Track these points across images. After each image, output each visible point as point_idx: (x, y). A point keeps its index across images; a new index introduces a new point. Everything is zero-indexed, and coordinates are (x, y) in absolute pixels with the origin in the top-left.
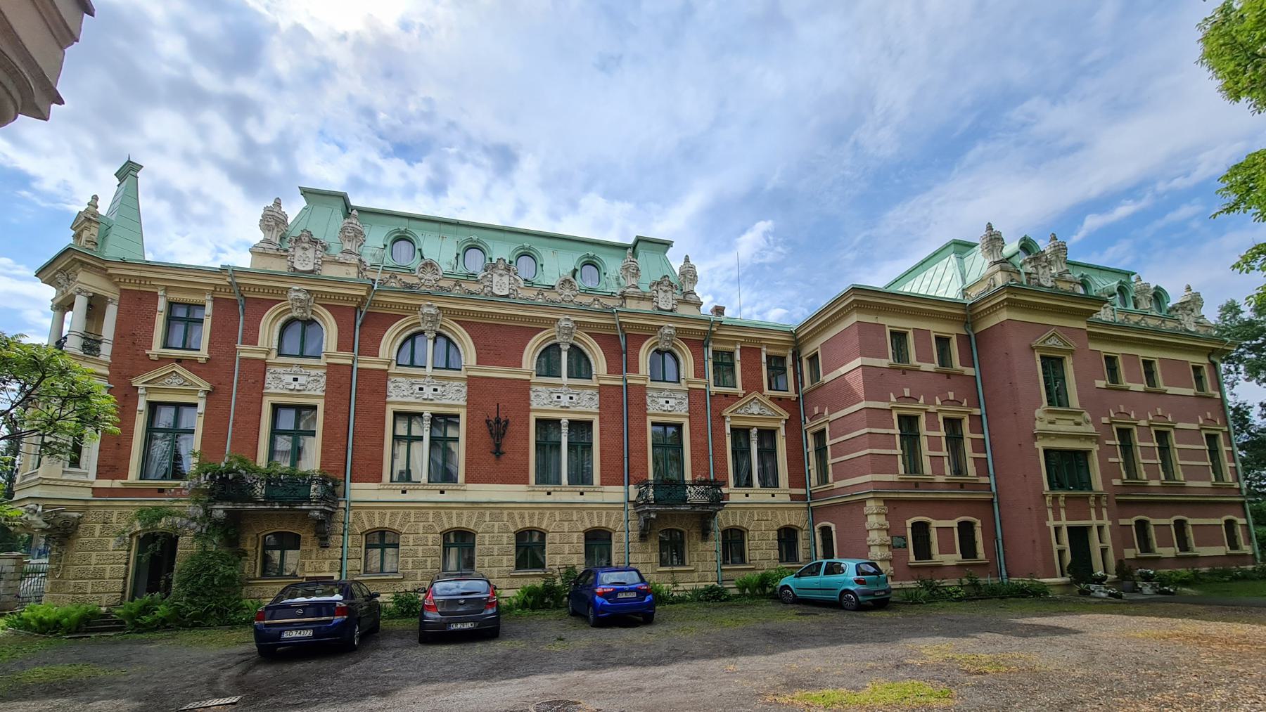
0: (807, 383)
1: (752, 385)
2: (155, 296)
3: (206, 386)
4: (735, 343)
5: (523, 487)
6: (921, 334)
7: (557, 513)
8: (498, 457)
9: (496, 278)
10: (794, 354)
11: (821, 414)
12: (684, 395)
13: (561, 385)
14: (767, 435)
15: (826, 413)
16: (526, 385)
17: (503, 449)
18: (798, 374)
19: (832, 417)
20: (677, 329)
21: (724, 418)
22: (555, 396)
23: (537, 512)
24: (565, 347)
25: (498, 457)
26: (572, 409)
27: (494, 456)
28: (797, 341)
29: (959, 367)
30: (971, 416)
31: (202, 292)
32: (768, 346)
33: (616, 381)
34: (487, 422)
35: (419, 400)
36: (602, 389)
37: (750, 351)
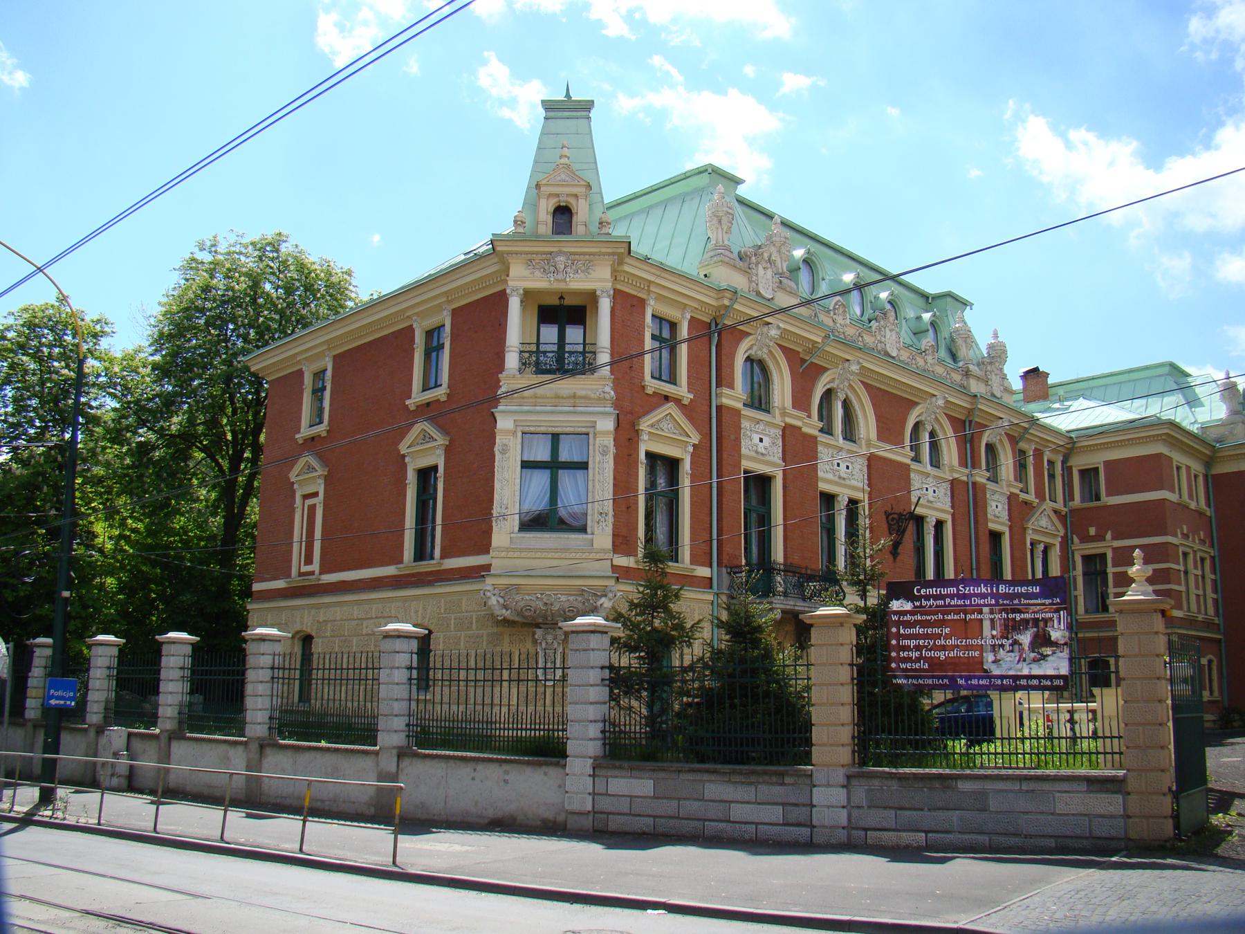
1: (1040, 495)
2: (642, 303)
3: (695, 438)
6: (1188, 468)
8: (895, 558)
9: (888, 334)
10: (1063, 462)
15: (1109, 536)
16: (906, 468)
18: (1068, 485)
21: (1025, 529)
25: (895, 558)
26: (935, 505)
27: (891, 558)
28: (1072, 449)
33: (962, 474)
34: (887, 515)
35: (836, 479)
36: (954, 483)
37: (1038, 454)
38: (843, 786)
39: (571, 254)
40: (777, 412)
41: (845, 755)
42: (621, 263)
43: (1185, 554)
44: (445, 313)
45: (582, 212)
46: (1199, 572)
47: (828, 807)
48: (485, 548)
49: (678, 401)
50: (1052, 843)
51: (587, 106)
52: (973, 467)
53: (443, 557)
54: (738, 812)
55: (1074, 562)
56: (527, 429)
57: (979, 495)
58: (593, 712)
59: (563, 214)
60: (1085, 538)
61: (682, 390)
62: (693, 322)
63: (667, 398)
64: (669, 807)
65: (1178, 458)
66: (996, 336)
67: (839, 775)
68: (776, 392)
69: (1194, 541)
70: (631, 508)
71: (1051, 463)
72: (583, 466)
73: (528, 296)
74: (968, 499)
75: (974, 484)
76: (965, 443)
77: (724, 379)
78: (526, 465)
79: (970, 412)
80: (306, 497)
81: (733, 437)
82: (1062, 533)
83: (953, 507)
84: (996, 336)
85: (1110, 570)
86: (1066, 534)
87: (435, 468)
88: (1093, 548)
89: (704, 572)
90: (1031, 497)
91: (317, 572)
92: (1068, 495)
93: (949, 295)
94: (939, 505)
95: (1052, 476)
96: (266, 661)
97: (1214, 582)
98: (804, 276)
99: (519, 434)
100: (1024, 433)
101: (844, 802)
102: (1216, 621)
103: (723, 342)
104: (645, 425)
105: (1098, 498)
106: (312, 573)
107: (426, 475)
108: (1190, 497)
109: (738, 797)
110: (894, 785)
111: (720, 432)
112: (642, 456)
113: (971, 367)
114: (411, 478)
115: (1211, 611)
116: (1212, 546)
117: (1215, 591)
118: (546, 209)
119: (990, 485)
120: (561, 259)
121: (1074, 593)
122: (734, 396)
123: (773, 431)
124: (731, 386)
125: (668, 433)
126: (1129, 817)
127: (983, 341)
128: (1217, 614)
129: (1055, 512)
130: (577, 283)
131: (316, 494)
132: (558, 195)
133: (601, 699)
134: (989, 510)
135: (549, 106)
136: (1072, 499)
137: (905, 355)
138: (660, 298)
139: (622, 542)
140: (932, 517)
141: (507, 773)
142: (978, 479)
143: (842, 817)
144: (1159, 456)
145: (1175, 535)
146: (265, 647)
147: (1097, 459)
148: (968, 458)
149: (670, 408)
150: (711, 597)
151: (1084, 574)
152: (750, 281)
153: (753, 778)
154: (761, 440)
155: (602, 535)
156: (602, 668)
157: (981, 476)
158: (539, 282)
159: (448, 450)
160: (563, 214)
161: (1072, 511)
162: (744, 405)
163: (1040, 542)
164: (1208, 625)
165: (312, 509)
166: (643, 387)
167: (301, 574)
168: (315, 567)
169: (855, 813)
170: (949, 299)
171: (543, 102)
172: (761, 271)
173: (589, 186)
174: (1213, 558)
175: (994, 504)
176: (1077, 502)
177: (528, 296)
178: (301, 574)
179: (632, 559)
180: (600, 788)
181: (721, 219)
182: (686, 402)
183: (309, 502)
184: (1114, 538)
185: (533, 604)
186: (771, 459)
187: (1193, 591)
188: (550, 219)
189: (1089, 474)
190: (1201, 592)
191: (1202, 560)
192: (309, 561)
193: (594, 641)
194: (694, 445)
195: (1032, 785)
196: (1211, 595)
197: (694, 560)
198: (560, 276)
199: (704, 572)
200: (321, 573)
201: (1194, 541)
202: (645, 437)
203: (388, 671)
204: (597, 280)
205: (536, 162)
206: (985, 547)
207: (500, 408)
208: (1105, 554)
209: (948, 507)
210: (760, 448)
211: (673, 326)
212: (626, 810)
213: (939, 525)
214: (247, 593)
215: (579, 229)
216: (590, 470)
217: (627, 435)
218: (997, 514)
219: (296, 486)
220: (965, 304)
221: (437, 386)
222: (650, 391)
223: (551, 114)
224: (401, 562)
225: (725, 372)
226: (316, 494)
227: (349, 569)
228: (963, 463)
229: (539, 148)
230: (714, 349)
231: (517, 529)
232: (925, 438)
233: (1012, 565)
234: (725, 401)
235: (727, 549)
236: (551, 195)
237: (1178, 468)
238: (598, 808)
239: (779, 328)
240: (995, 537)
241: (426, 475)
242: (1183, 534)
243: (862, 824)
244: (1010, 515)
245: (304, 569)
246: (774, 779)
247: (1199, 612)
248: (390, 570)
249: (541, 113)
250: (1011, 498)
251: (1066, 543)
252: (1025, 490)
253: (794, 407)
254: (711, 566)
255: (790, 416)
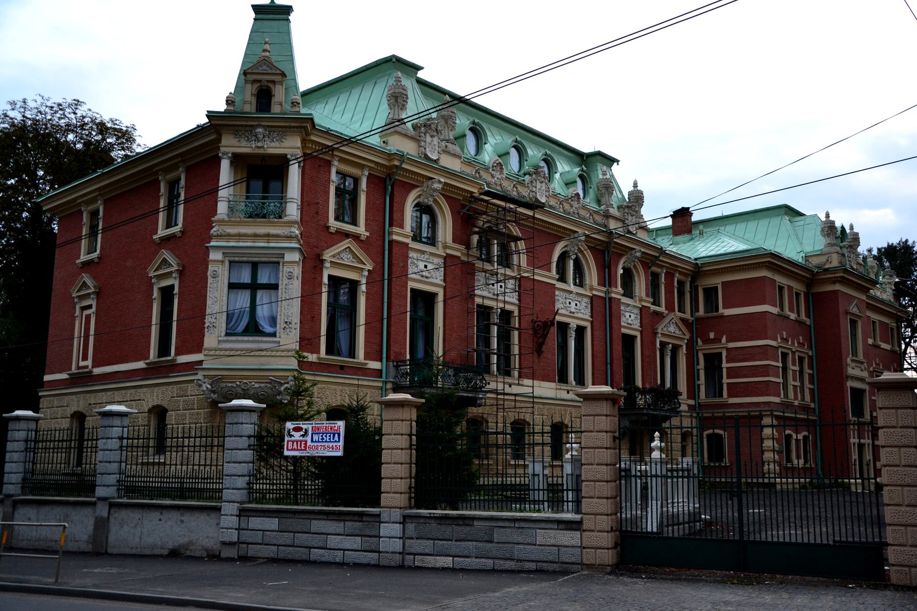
0: (701, 312)
3: (369, 267)
4: (661, 267)
5: (553, 385)
6: (790, 288)
7: (573, 410)
9: (539, 185)
10: (691, 283)
11: (717, 340)
12: (637, 311)
13: (571, 292)
14: (676, 348)
15: (724, 340)
17: (544, 348)
19: (731, 345)
20: (643, 253)
21: (656, 333)
22: (568, 301)
23: (563, 408)
24: (574, 257)
26: (576, 315)
29: (804, 318)
30: (809, 356)
31: (362, 167)
32: (680, 273)
38: (400, 523)
39: (268, 126)
40: (440, 245)
41: (401, 500)
42: (308, 134)
43: (785, 355)
44: (181, 169)
45: (279, 94)
46: (797, 368)
47: (390, 538)
48: (198, 347)
49: (356, 237)
50: (532, 566)
51: (288, 10)
52: (610, 286)
53: (177, 354)
54: (333, 541)
55: (698, 359)
56: (233, 259)
57: (614, 307)
58: (244, 468)
59: (264, 97)
60: (707, 341)
61: (361, 229)
62: (370, 177)
63: (347, 235)
64: (287, 538)
65: (780, 279)
66: (635, 185)
67: (397, 515)
68: (440, 230)
69: (793, 343)
70: (316, 318)
71: (680, 283)
72: (275, 287)
73: (237, 160)
74: (605, 311)
75: (610, 299)
76: (604, 268)
77: (396, 220)
78: (232, 286)
79: (608, 244)
80: (83, 308)
81: (401, 265)
82: (687, 337)
83: (592, 317)
84: (635, 185)
85: (725, 365)
86: (692, 337)
87: (172, 287)
88: (712, 348)
89: (374, 365)
90: (662, 309)
91: (90, 367)
92: (695, 308)
93: (599, 154)
94: (580, 315)
95: (681, 294)
96: (22, 435)
97: (811, 376)
98: (470, 140)
99: (227, 264)
100: (653, 259)
101: (399, 534)
102: (812, 405)
103: (395, 193)
104: (328, 255)
105: (717, 310)
106: (87, 367)
107: (167, 293)
108: (791, 310)
109: (331, 530)
110: (434, 524)
111: (389, 260)
112: (325, 280)
113: (611, 210)
114: (156, 294)
115: (808, 398)
116: (810, 348)
117: (811, 382)
118: (250, 90)
119: (625, 300)
120: (260, 130)
121: (697, 382)
122: (402, 234)
123: (436, 260)
124: (401, 226)
125: (344, 261)
126: (584, 548)
127: (626, 188)
128: (813, 400)
129: (682, 320)
130: (273, 147)
131: (90, 307)
132: (260, 81)
133: (248, 460)
134: (623, 319)
135: (257, 9)
136: (697, 310)
137: (553, 202)
138: (342, 160)
139: (308, 342)
140: (573, 323)
141: (182, 515)
142: (613, 295)
143: (397, 545)
144: (763, 278)
145: (775, 339)
146: (23, 425)
147: (717, 281)
148: (606, 279)
149: (347, 243)
150: (381, 385)
151: (706, 369)
152: (420, 146)
153: (342, 518)
154: (426, 266)
155: (290, 339)
156: (249, 437)
157: (617, 292)
158: (245, 147)
159: (181, 273)
160: (264, 97)
161: (699, 320)
162: (412, 240)
163: (669, 343)
164: (805, 408)
165: (88, 317)
166: (328, 227)
167: (79, 368)
168: (89, 363)
169: (408, 542)
170: (599, 157)
171: (253, 6)
172: (428, 139)
173: (283, 75)
174: (810, 358)
175: (627, 314)
176: (701, 312)
177: (237, 160)
178: (79, 368)
179: (315, 356)
180: (243, 525)
181: (397, 99)
182: (363, 238)
183: (86, 312)
184: (728, 341)
185: (234, 390)
186: (434, 281)
187: (791, 382)
188: (254, 100)
189: (711, 293)
190: (798, 384)
191: (801, 359)
192: (85, 358)
193: (243, 417)
194: (369, 271)
195: (522, 525)
196: (807, 385)
197: (368, 356)
198: (260, 144)
199: (374, 365)
200: (93, 367)
201: (793, 343)
202: (327, 265)
203: (104, 441)
204: (291, 146)
205: (246, 54)
206: (618, 347)
207: (212, 244)
208: (721, 354)
209: (588, 317)
210: (425, 271)
211: (356, 181)
212: (260, 541)
213: (580, 330)
214: (42, 384)
215: (276, 109)
216: (280, 291)
217: (313, 264)
218: (630, 321)
219: (76, 300)
220: (610, 161)
221: (176, 225)
222: (332, 230)
223: (260, 16)
224: (148, 358)
225: (395, 216)
226: (90, 307)
227: (113, 364)
228: (602, 283)
229: (248, 43)
230: (388, 198)
231: (223, 333)
232: (571, 264)
233: (642, 361)
234: (395, 237)
235: (394, 348)
236: (254, 81)
237: (781, 288)
238: (242, 539)
239: (440, 182)
240: (629, 341)
241: (167, 293)
242: (782, 338)
243: (412, 551)
244: (641, 323)
245: (82, 364)
246: (356, 518)
247: (796, 398)
248: (140, 365)
249: (253, 15)
250: (643, 310)
251: (691, 345)
252: (656, 303)
253: (454, 241)
254: (381, 361)
255: (450, 248)
